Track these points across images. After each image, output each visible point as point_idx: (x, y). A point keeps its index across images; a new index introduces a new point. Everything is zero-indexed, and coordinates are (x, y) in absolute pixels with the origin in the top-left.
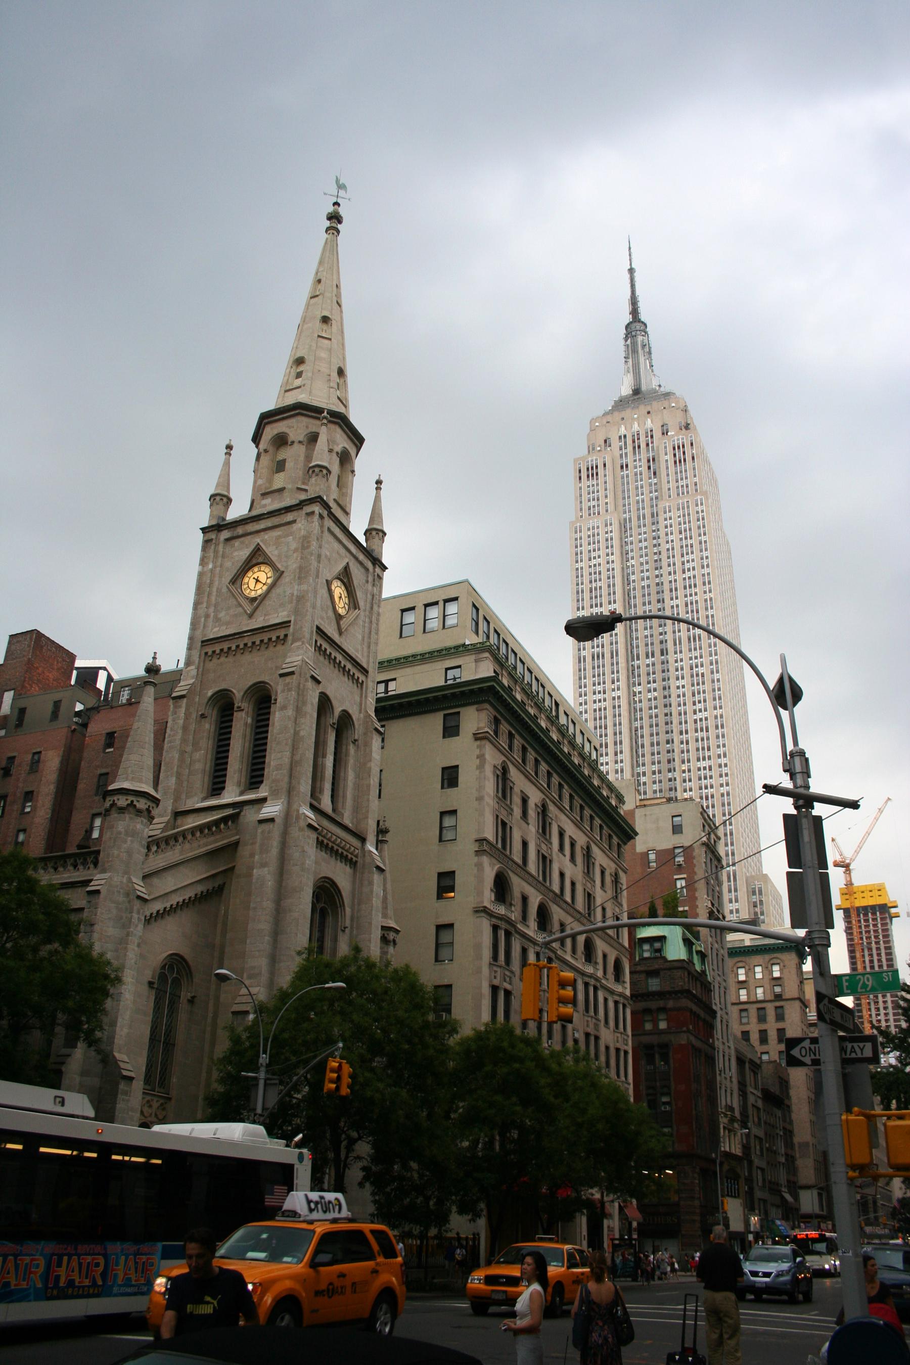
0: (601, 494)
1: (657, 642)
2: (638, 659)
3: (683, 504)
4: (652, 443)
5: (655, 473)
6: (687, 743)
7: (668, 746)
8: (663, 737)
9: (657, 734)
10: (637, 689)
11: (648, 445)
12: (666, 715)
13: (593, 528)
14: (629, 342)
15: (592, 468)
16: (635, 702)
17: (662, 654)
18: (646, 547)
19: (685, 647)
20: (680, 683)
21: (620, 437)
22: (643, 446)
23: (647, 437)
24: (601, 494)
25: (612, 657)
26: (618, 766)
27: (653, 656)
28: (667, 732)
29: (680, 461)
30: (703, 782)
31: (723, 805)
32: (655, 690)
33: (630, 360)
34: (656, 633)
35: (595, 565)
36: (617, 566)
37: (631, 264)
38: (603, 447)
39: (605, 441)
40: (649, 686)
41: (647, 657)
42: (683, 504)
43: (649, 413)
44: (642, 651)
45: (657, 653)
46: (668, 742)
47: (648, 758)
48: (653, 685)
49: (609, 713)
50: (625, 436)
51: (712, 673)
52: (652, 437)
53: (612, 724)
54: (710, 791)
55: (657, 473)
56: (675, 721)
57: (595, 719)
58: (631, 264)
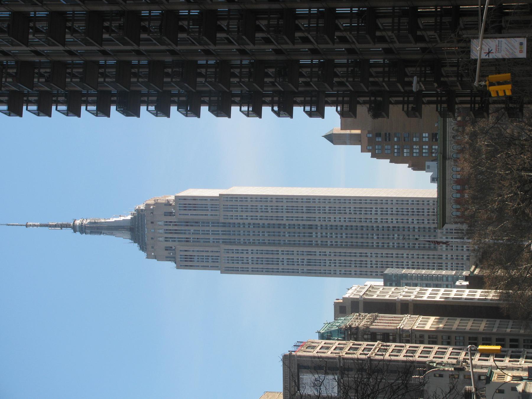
0: (205, 254)
1: (303, 231)
2: (312, 241)
3: (224, 208)
4: (175, 222)
5: (197, 223)
6: (366, 219)
7: (364, 229)
8: (359, 232)
9: (357, 234)
10: (329, 243)
11: (176, 225)
12: (346, 229)
13: (228, 260)
14: (89, 231)
15: (186, 258)
16: (337, 245)
17: (311, 228)
18: (244, 232)
19: (313, 215)
20: (332, 219)
21: (166, 241)
22: (176, 228)
23: (170, 225)
24: (205, 254)
25: (311, 255)
26: (374, 255)
27: (312, 233)
28: (357, 229)
29: (185, 207)
30: (389, 212)
31: (402, 204)
32: (331, 234)
33: (103, 231)
34: (298, 230)
35: (252, 261)
36: (255, 248)
37: (24, 225)
38: (170, 251)
39: (166, 250)
40: (328, 237)
41: (312, 236)
42: (224, 208)
43: (152, 223)
44: (308, 239)
45: (310, 231)
46: (362, 229)
47: (370, 241)
48: (329, 235)
49: (343, 259)
50: (166, 238)
51: (330, 202)
52: (171, 222)
53: (349, 257)
54: (394, 210)
55: (197, 221)
56: (354, 224)
57: (345, 266)
58: (24, 225)
